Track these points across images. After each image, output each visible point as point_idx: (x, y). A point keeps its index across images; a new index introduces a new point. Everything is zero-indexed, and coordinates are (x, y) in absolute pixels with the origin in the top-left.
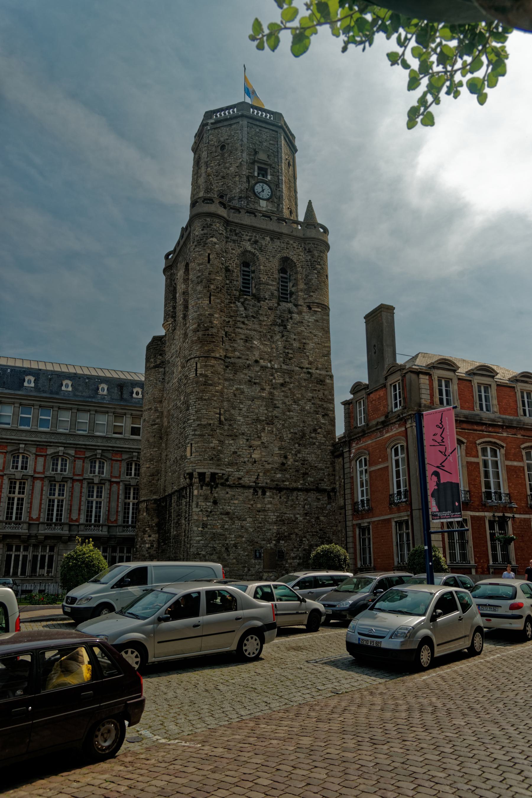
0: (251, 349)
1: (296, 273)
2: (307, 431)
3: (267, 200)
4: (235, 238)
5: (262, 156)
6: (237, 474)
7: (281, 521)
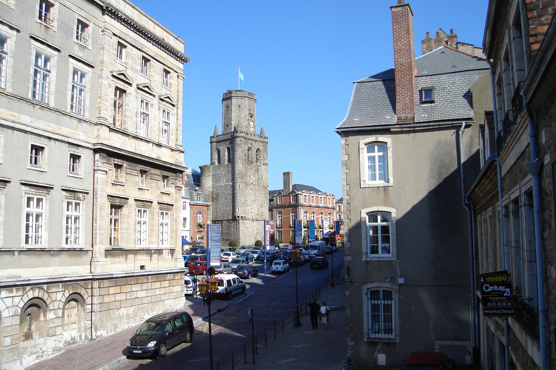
0: (250, 179)
1: (261, 153)
2: (263, 203)
3: (253, 127)
4: (247, 143)
5: (251, 112)
6: (248, 217)
7: (257, 229)
